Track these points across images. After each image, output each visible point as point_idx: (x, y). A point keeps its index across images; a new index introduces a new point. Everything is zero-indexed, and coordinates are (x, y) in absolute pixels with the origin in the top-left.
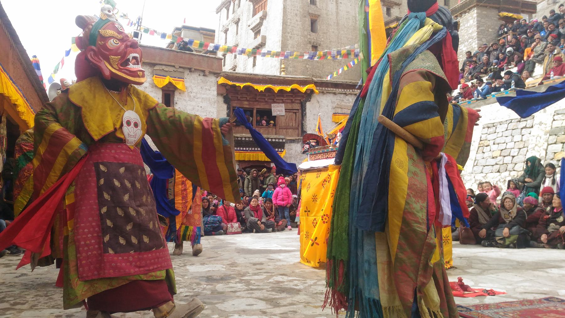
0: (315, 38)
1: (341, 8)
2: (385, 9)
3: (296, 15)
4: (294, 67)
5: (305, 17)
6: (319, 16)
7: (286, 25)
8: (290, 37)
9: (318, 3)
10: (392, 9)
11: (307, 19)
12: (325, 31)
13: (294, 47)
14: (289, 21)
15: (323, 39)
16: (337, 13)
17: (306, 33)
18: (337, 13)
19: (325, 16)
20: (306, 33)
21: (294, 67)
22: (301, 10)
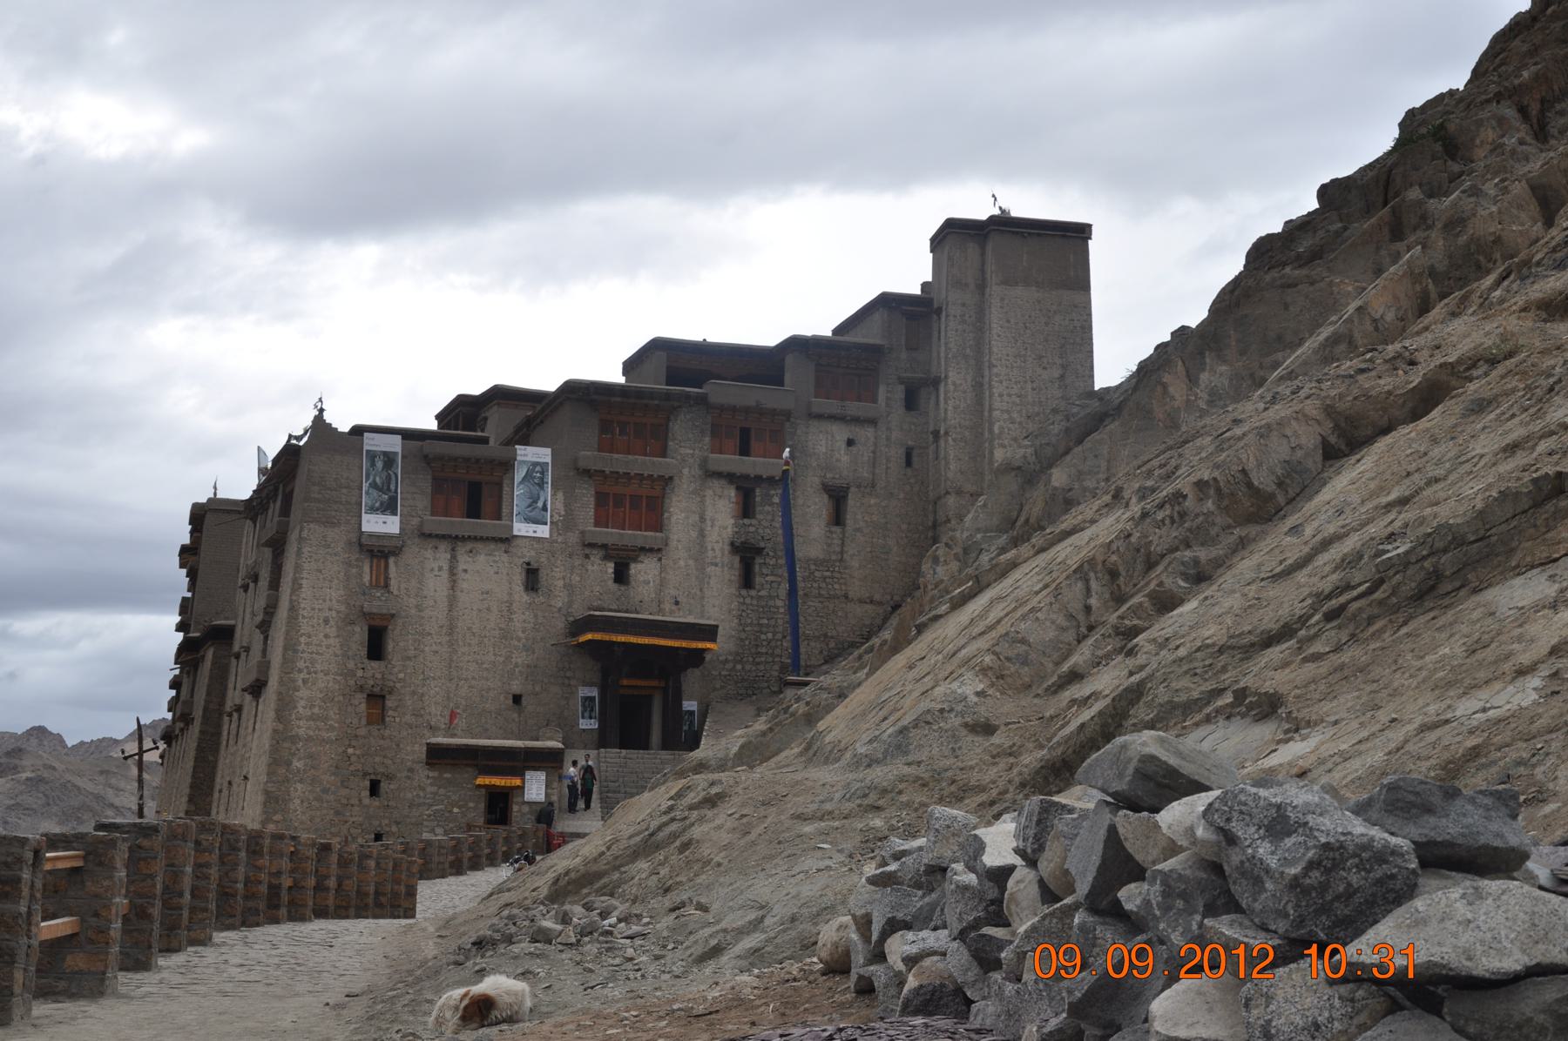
0: (379, 676)
1: (465, 585)
2: (610, 567)
3: (326, 621)
4: (311, 756)
5: (352, 623)
6: (393, 616)
7: (296, 651)
8: (305, 681)
9: (393, 583)
10: (633, 566)
11: (357, 629)
12: (412, 653)
13: (312, 706)
14: (302, 640)
15: (401, 676)
16: (452, 602)
17: (351, 665)
18: (452, 602)
19: (413, 611)
20: (351, 665)
21: (311, 756)
22: (343, 608)
